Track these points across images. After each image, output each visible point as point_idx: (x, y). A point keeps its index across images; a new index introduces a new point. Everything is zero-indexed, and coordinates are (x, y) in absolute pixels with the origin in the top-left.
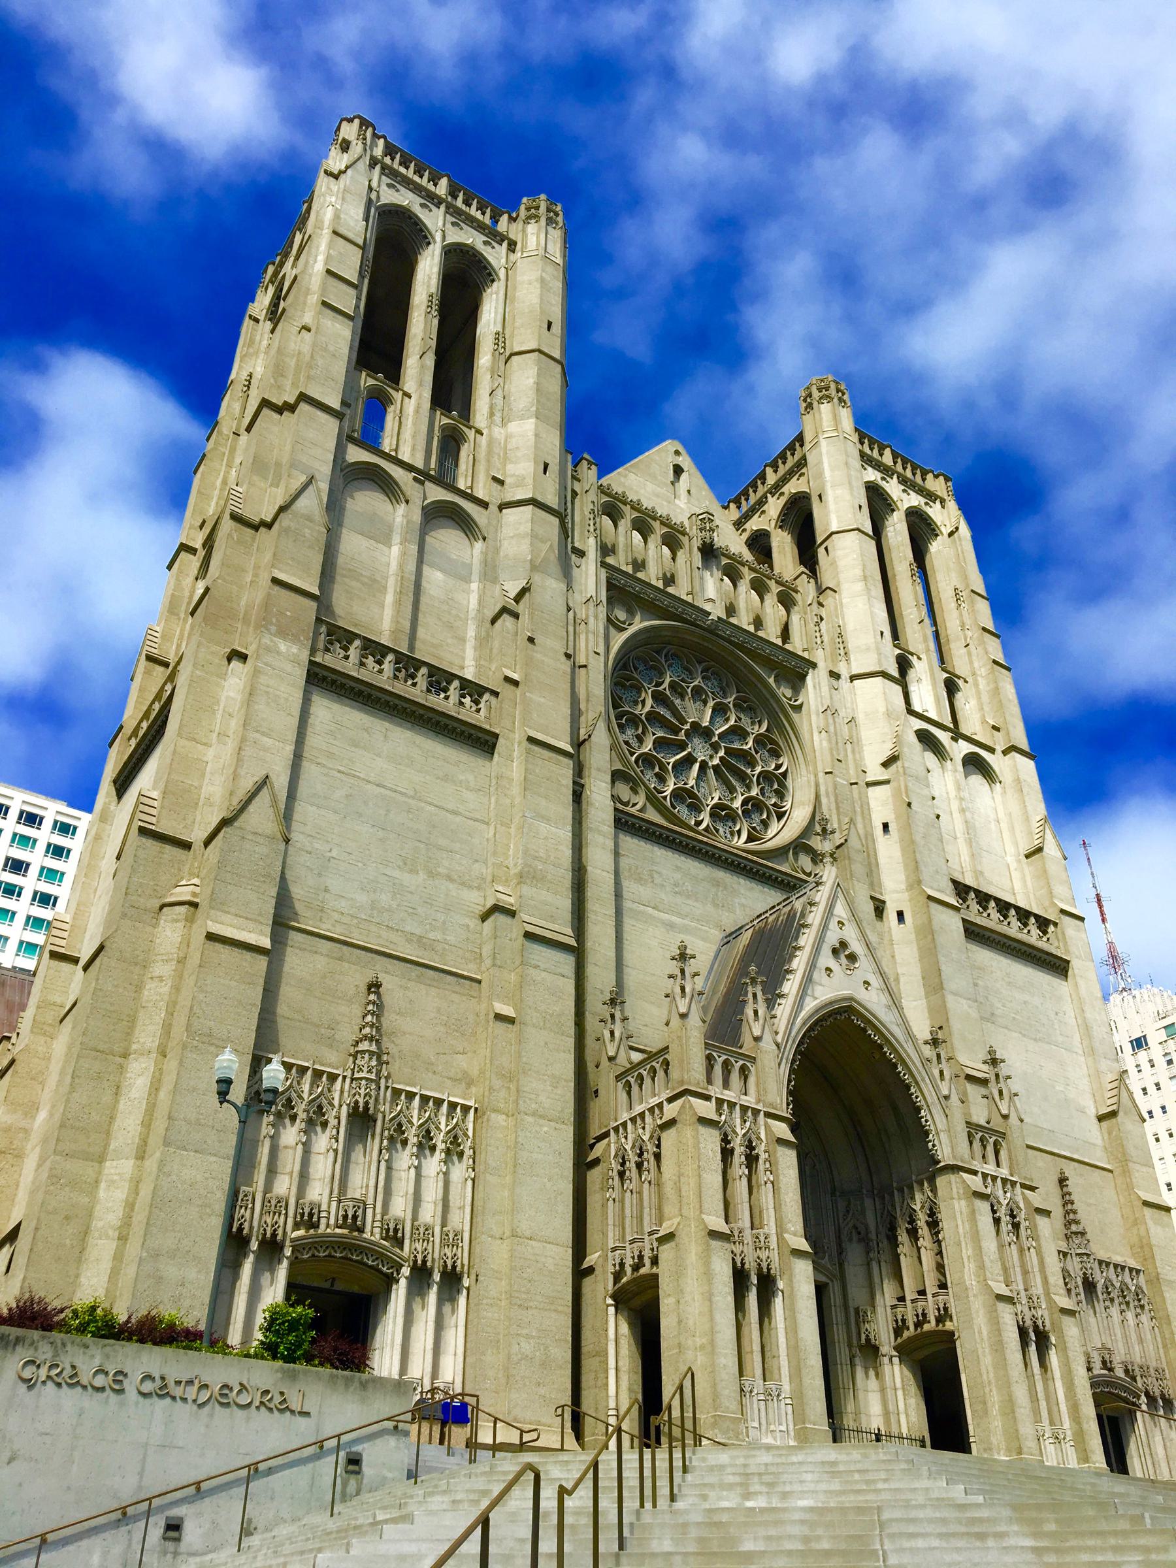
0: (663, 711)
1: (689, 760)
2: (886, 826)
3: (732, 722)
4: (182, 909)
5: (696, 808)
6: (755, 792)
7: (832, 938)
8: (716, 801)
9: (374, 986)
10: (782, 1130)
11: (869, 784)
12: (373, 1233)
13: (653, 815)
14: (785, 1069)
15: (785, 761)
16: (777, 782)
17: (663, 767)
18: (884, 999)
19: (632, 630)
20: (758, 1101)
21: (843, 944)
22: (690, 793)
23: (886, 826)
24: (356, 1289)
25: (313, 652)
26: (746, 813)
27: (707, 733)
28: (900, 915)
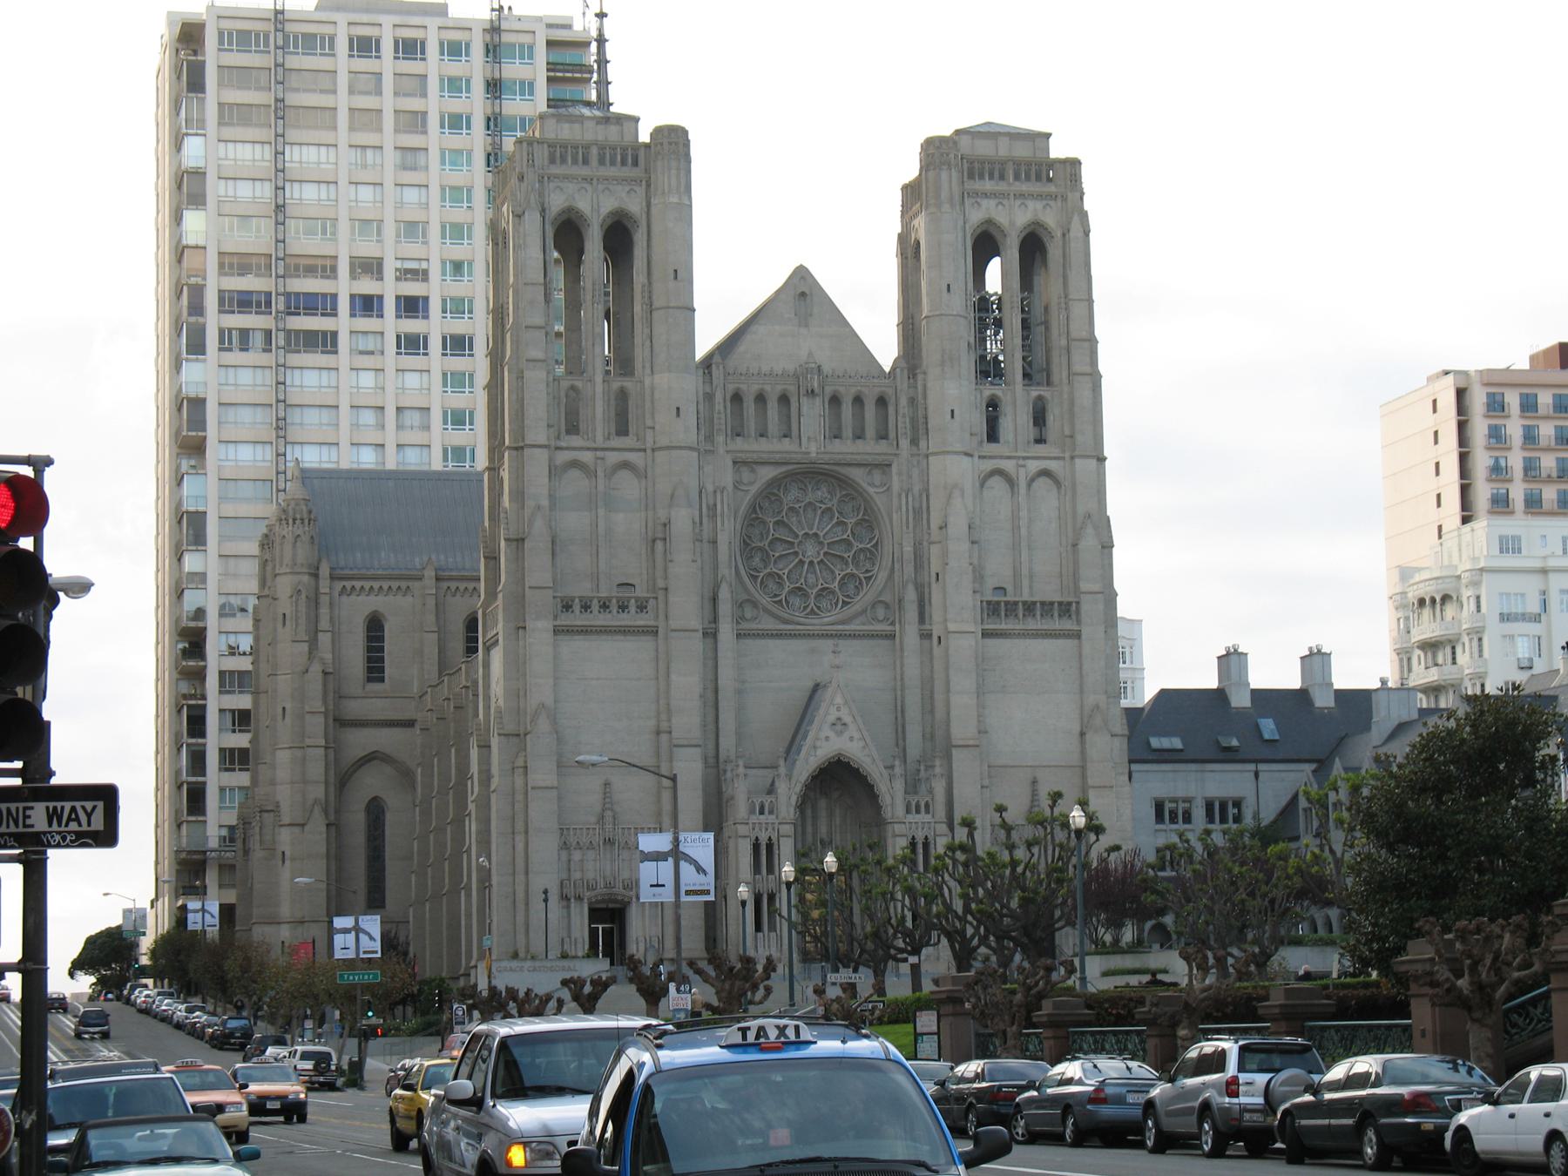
0: (782, 534)
1: (801, 562)
2: (937, 574)
3: (835, 520)
4: (521, 770)
5: (806, 595)
6: (851, 569)
7: (832, 718)
8: (820, 587)
9: (607, 784)
10: (788, 829)
11: (930, 543)
12: (619, 889)
13: (769, 624)
14: (794, 799)
15: (876, 532)
16: (872, 554)
17: (780, 577)
18: (862, 744)
19: (754, 489)
20: (777, 817)
21: (839, 719)
22: (799, 589)
23: (937, 574)
24: (618, 906)
25: (555, 618)
26: (842, 584)
27: (816, 535)
28: (939, 638)
